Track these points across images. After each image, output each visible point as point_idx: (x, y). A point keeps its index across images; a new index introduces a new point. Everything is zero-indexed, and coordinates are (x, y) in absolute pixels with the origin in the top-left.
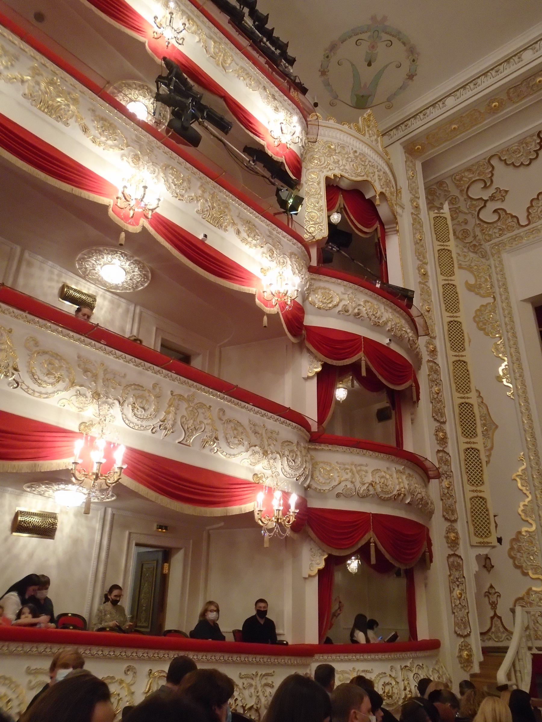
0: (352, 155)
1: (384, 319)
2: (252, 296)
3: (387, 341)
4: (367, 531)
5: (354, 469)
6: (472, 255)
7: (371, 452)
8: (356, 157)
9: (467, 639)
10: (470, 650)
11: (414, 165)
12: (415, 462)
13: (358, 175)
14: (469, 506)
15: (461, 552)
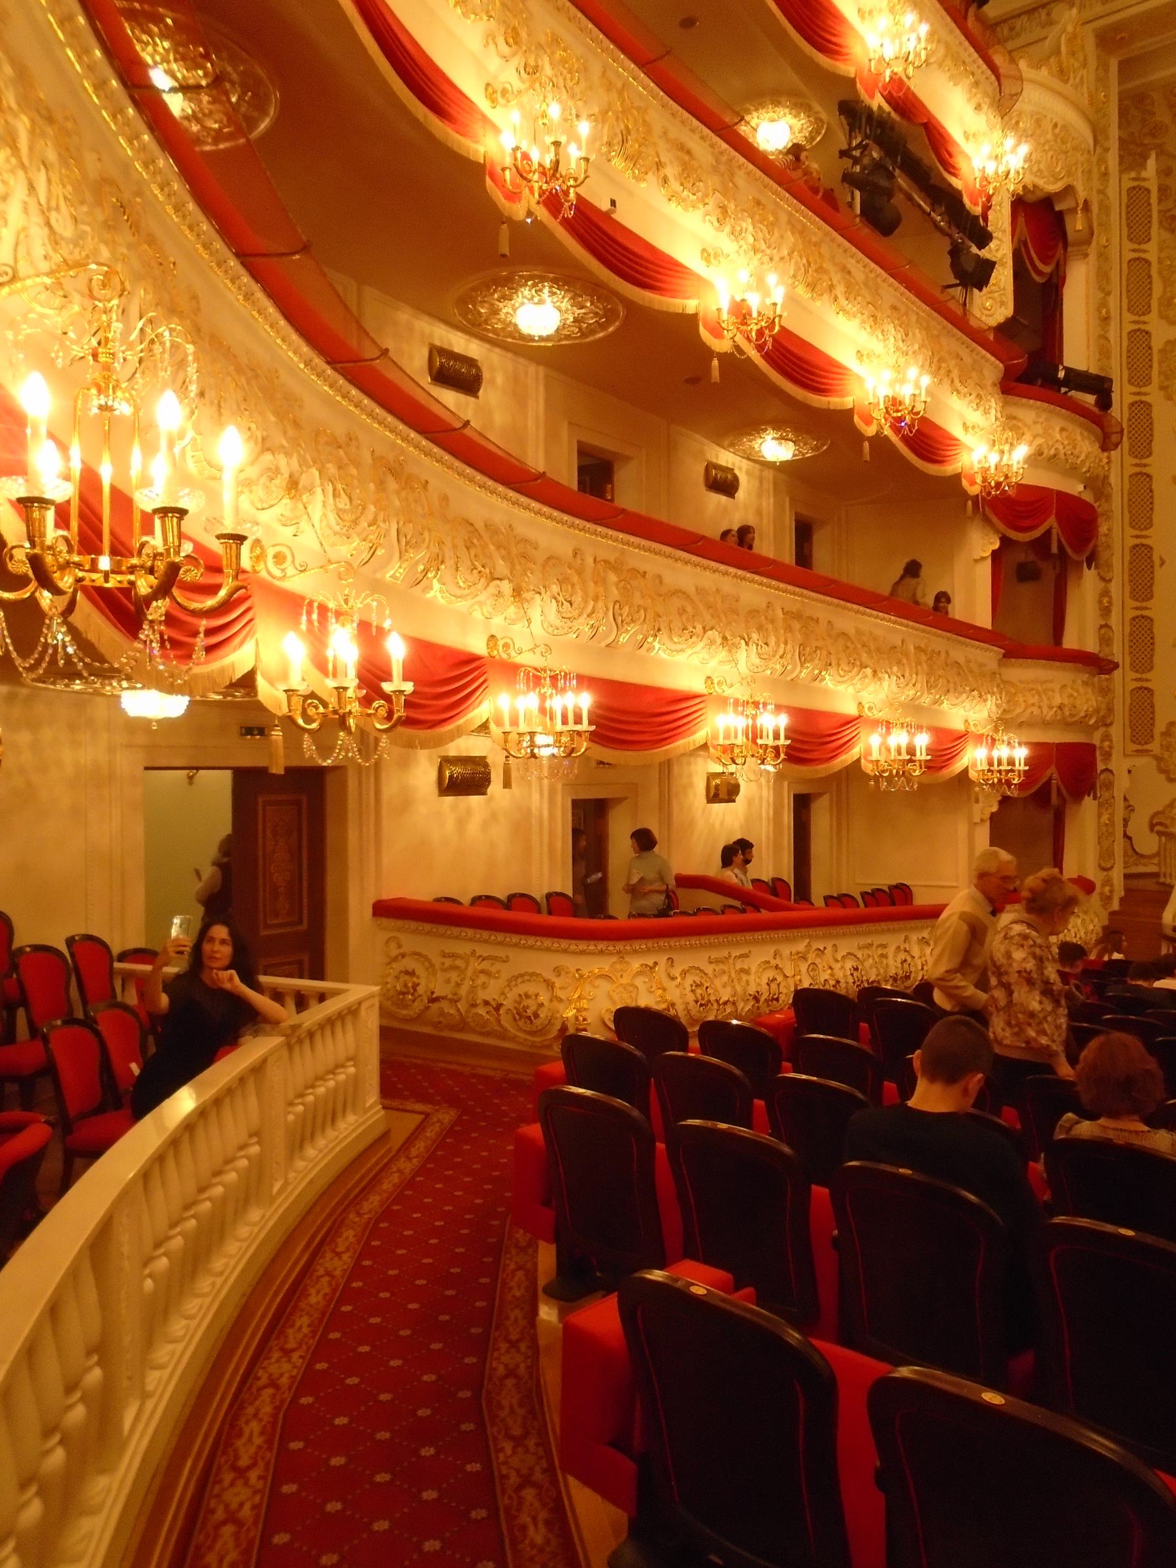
0: (1050, 136)
1: (1083, 457)
2: (957, 477)
3: (1081, 488)
4: (1048, 767)
5: (1040, 688)
6: (1166, 235)
7: (1058, 664)
8: (1056, 136)
9: (1110, 873)
10: (1112, 886)
11: (1107, 71)
12: (1096, 664)
13: (1057, 180)
14: (1128, 701)
15: (1112, 766)
